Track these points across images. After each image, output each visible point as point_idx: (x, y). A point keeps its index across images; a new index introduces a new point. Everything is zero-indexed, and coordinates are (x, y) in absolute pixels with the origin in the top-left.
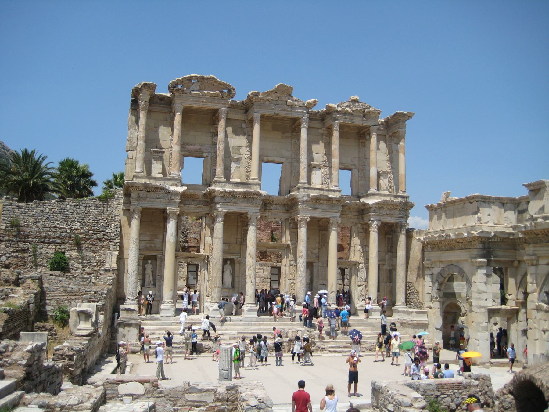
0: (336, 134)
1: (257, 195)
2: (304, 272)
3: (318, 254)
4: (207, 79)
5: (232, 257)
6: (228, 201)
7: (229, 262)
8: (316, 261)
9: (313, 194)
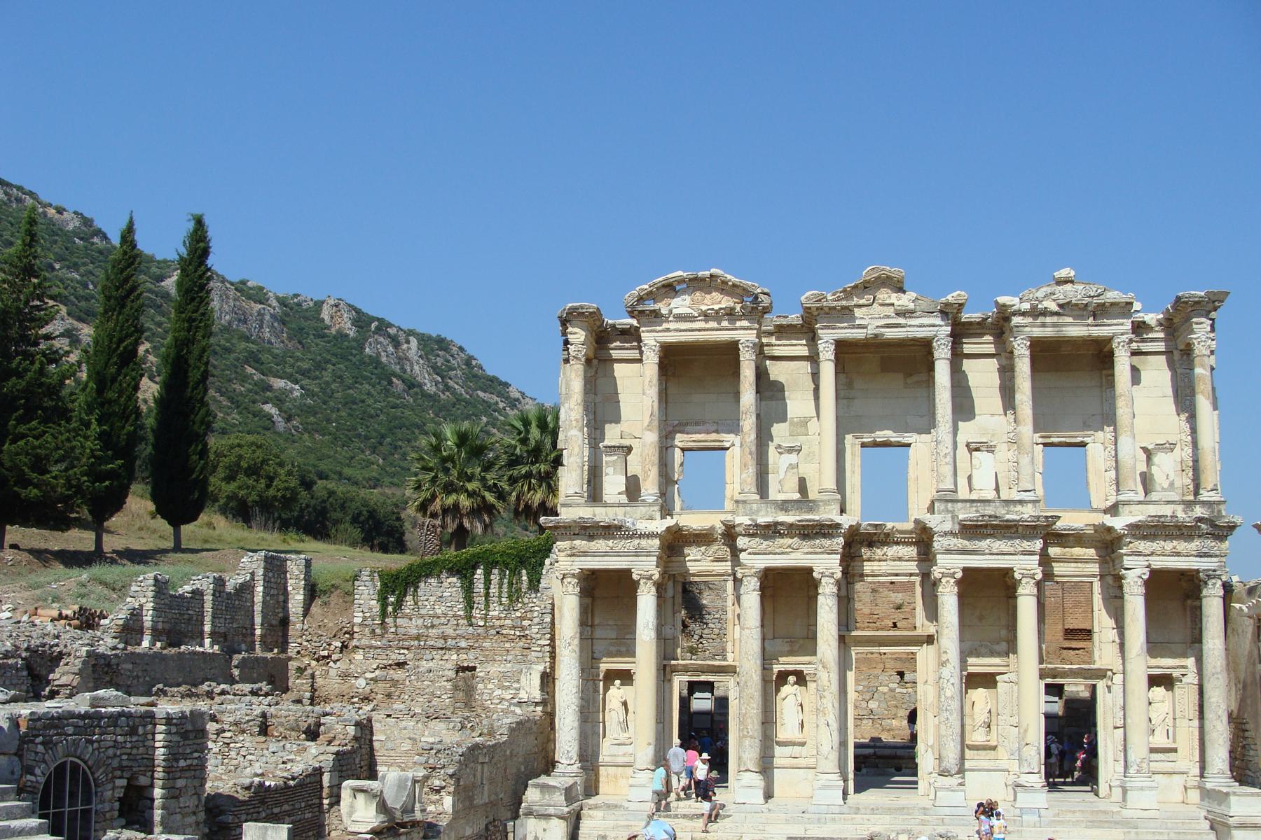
0: (1023, 367)
2: (952, 697)
5: (798, 667)
7: (792, 679)
9: (967, 514)
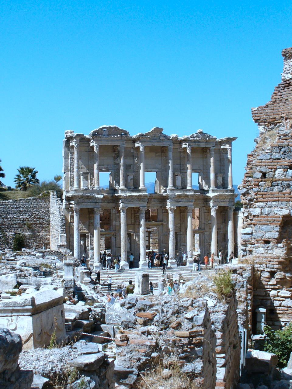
1: (145, 196)
3: (180, 227)
4: (113, 128)
6: (128, 201)
8: (179, 231)
